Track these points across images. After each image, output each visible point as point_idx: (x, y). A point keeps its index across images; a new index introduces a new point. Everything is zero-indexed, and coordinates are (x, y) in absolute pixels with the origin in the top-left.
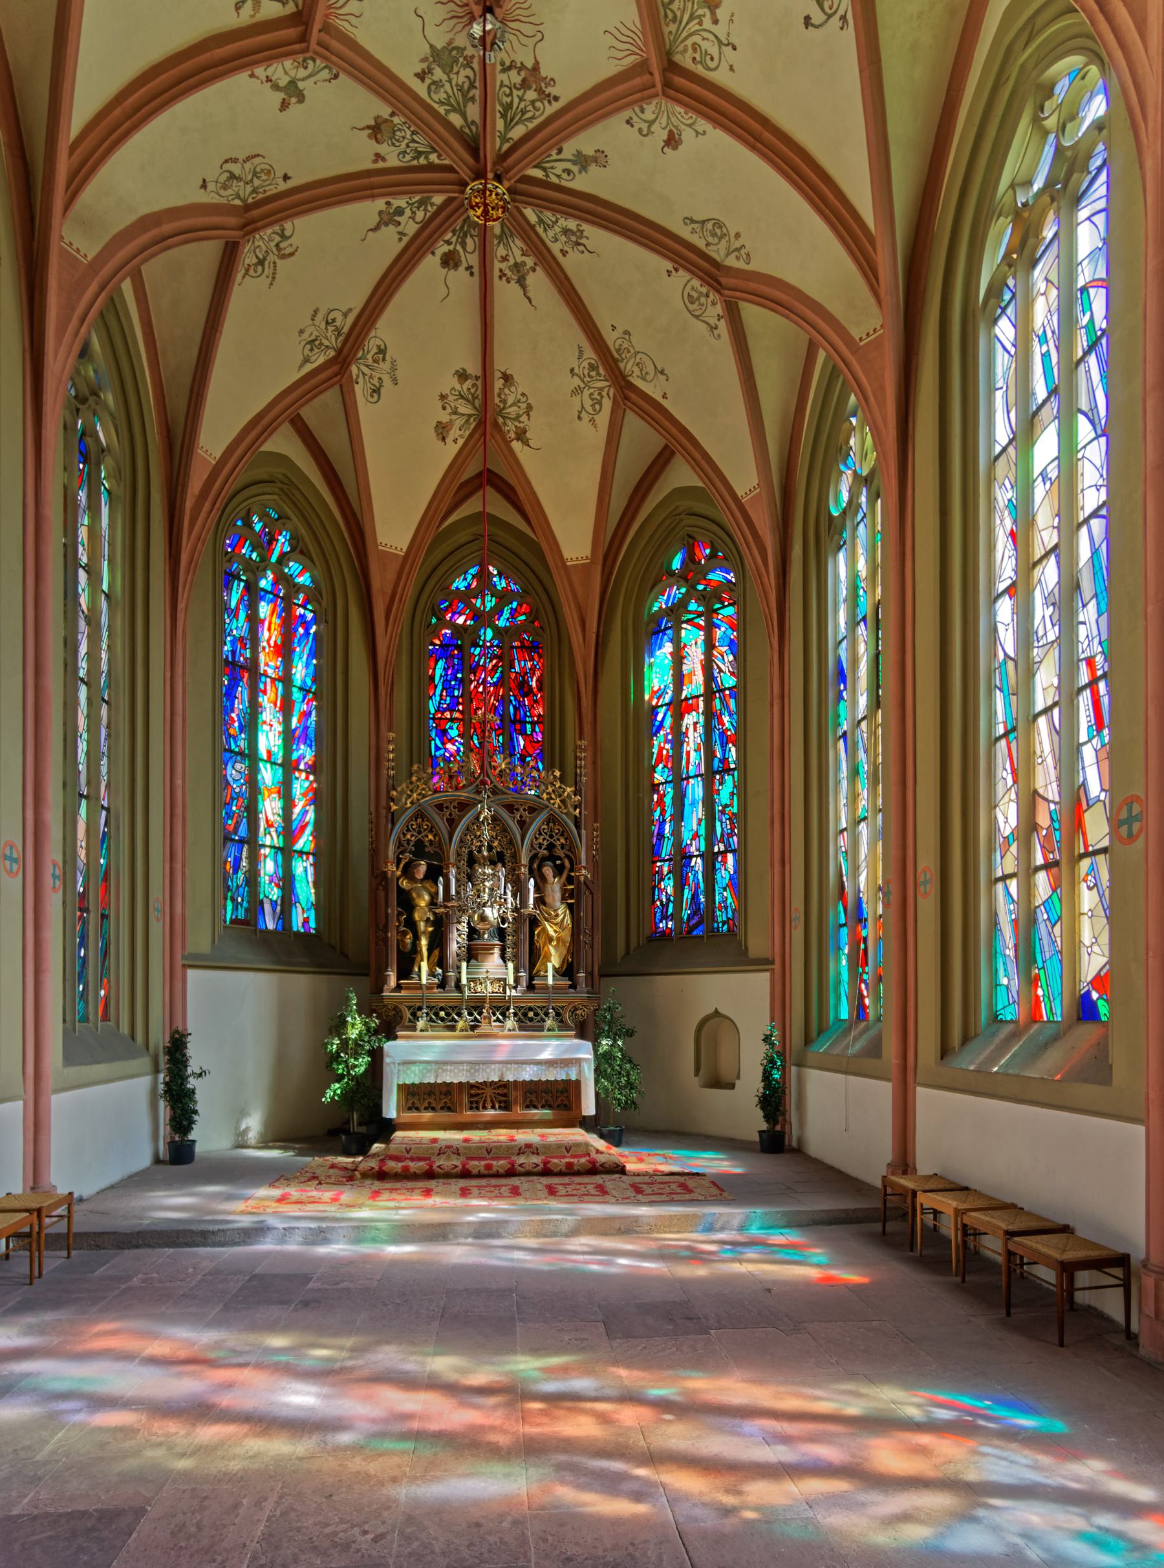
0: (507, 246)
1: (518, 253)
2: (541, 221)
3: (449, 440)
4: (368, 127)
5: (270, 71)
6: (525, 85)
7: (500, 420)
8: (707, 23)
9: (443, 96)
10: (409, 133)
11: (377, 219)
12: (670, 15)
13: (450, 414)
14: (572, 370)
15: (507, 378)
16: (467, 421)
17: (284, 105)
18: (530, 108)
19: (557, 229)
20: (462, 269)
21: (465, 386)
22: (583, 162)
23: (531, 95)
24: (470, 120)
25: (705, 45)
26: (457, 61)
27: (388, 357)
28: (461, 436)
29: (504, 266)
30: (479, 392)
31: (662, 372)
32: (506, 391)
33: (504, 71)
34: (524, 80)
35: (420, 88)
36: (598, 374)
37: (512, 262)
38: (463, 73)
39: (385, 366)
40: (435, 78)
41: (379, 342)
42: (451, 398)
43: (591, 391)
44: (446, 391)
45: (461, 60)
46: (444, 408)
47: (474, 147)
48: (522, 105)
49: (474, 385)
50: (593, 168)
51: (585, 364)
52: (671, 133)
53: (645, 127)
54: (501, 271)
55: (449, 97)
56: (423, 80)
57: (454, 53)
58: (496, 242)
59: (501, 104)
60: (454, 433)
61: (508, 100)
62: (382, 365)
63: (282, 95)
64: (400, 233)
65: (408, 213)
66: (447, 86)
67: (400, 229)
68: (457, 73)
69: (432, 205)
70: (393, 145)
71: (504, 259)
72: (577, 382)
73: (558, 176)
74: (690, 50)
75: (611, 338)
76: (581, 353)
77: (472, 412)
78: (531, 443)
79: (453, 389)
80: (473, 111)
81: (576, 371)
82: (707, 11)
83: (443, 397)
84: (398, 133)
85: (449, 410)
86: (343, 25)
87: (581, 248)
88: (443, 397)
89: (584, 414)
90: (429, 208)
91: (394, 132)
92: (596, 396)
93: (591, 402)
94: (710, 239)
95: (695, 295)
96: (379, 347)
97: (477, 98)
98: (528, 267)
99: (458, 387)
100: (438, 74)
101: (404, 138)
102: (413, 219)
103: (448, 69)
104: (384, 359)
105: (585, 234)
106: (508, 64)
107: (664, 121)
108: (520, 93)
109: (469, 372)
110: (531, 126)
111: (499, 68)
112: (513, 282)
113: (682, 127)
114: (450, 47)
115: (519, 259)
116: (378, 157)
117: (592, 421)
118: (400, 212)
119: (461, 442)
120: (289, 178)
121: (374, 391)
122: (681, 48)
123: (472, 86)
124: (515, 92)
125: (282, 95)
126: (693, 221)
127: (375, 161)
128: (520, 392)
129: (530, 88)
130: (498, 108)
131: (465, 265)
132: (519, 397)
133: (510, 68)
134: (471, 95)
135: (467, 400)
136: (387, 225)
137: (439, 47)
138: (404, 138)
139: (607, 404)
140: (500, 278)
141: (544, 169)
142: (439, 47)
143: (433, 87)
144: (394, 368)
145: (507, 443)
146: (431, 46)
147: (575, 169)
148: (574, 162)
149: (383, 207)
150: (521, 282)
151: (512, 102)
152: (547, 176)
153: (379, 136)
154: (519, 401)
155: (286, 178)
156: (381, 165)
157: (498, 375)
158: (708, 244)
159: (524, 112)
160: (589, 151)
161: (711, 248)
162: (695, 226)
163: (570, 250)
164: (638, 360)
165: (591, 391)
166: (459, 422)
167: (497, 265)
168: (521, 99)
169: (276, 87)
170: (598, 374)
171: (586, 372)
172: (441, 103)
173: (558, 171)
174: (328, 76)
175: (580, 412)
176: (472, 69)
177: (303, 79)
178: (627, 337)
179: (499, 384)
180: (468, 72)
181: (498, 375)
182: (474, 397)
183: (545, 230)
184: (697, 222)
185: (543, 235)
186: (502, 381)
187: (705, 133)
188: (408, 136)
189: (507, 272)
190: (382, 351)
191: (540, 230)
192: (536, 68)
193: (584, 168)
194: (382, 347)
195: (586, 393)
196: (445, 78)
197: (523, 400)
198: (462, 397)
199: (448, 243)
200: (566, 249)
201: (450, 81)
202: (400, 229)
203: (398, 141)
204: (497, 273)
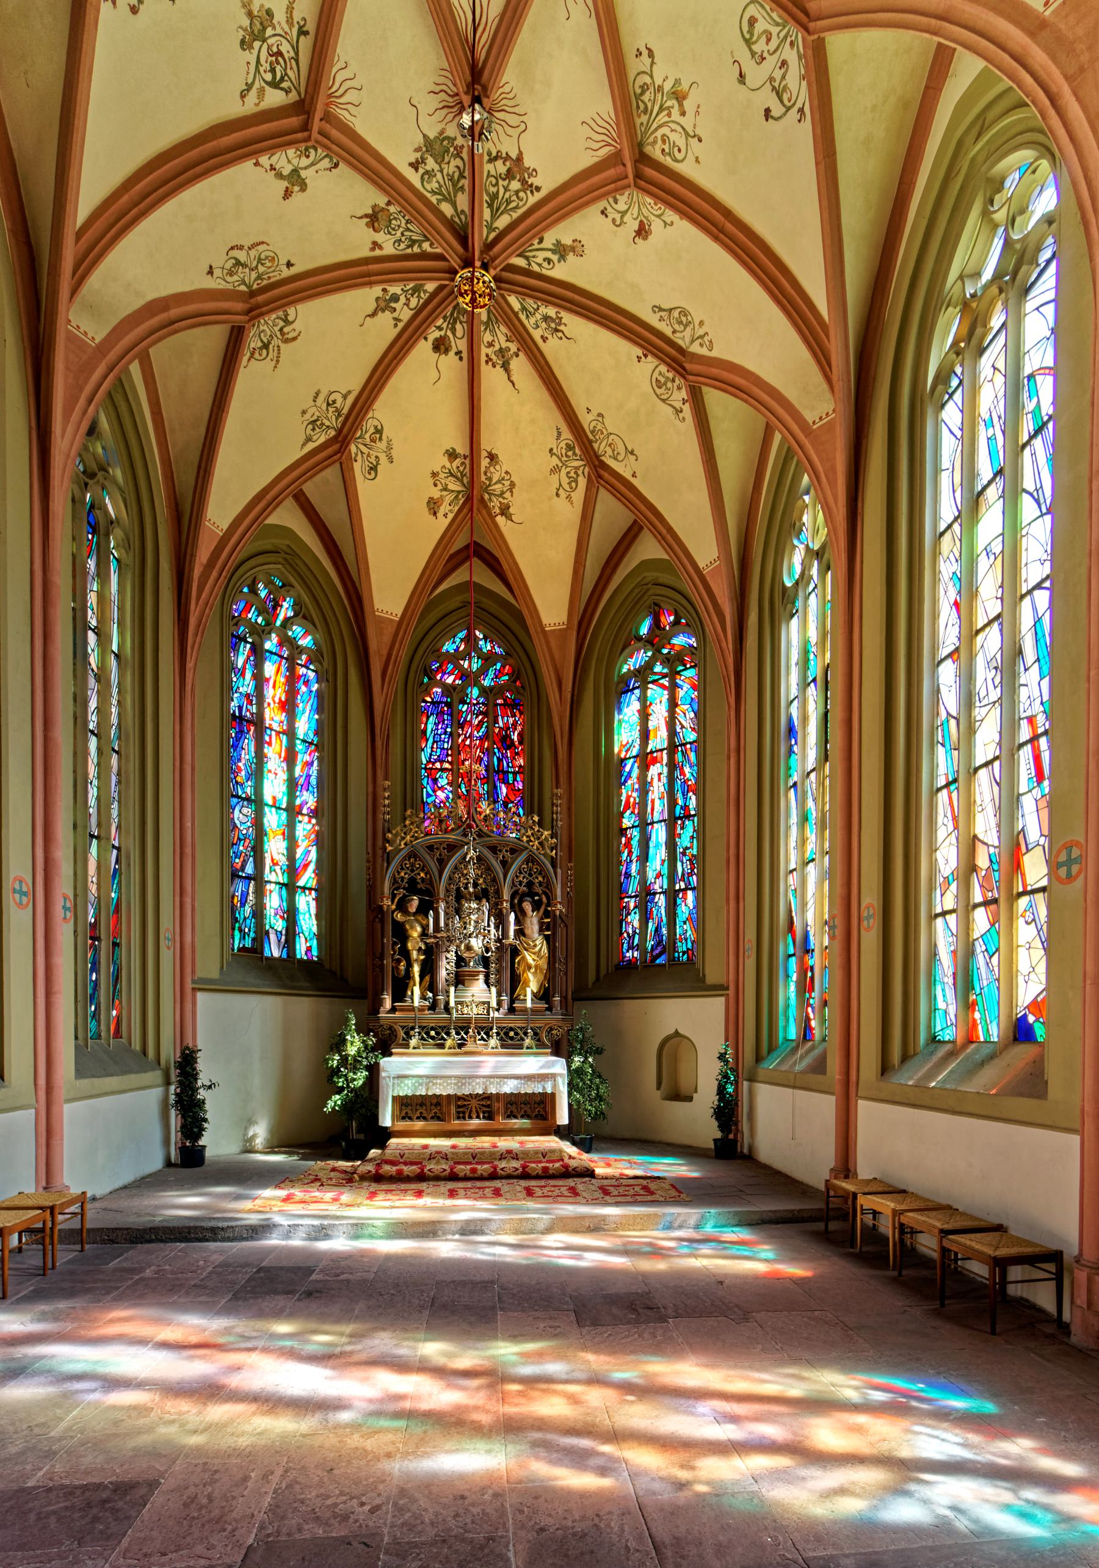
0: (493, 333)
1: (502, 339)
2: (524, 309)
4: (366, 216)
6: (509, 175)
7: (486, 496)
9: (435, 185)
15: (492, 457)
16: (456, 497)
17: (287, 194)
19: (538, 316)
20: (452, 353)
22: (562, 251)
23: (515, 185)
26: (448, 151)
27: (384, 437)
28: (451, 511)
30: (467, 470)
32: (492, 469)
33: (490, 161)
37: (497, 347)
38: (453, 163)
39: (382, 445)
41: (376, 423)
42: (442, 475)
44: (437, 469)
46: (435, 485)
47: (463, 237)
48: (507, 195)
49: (463, 463)
50: (571, 257)
54: (487, 355)
57: (445, 143)
58: (483, 328)
59: (488, 194)
61: (495, 190)
62: (378, 444)
63: (285, 184)
64: (395, 319)
65: (403, 299)
66: (439, 175)
67: (395, 315)
69: (425, 292)
71: (490, 345)
73: (540, 265)
79: (444, 467)
80: (463, 201)
83: (434, 475)
85: (440, 487)
86: (343, 114)
87: (560, 334)
88: (434, 475)
91: (390, 221)
96: (376, 427)
99: (448, 465)
102: (408, 305)
103: (440, 160)
104: (380, 439)
105: (563, 321)
106: (494, 154)
108: (506, 183)
110: (515, 215)
111: (486, 158)
112: (498, 367)
115: (504, 345)
116: (376, 245)
119: (451, 516)
120: (292, 265)
124: (501, 182)
127: (373, 249)
128: (504, 470)
129: (514, 178)
130: (486, 198)
131: (454, 350)
133: (496, 158)
140: (487, 362)
141: (527, 258)
144: (389, 447)
147: (555, 258)
148: (554, 252)
150: (506, 366)
152: (529, 264)
155: (289, 265)
156: (378, 252)
157: (484, 454)
163: (550, 337)
166: (449, 498)
167: (484, 350)
168: (506, 189)
169: (280, 176)
172: (433, 192)
173: (539, 260)
177: (306, 168)
179: (485, 462)
181: (484, 454)
182: (463, 476)
183: (527, 317)
185: (525, 322)
186: (488, 460)
189: (494, 357)
190: (379, 431)
191: (523, 317)
192: (520, 159)
193: (563, 258)
194: (379, 427)
196: (437, 167)
197: (507, 477)
198: (452, 475)
199: (440, 328)
200: (546, 335)
201: (441, 171)
202: (395, 315)
204: (483, 358)
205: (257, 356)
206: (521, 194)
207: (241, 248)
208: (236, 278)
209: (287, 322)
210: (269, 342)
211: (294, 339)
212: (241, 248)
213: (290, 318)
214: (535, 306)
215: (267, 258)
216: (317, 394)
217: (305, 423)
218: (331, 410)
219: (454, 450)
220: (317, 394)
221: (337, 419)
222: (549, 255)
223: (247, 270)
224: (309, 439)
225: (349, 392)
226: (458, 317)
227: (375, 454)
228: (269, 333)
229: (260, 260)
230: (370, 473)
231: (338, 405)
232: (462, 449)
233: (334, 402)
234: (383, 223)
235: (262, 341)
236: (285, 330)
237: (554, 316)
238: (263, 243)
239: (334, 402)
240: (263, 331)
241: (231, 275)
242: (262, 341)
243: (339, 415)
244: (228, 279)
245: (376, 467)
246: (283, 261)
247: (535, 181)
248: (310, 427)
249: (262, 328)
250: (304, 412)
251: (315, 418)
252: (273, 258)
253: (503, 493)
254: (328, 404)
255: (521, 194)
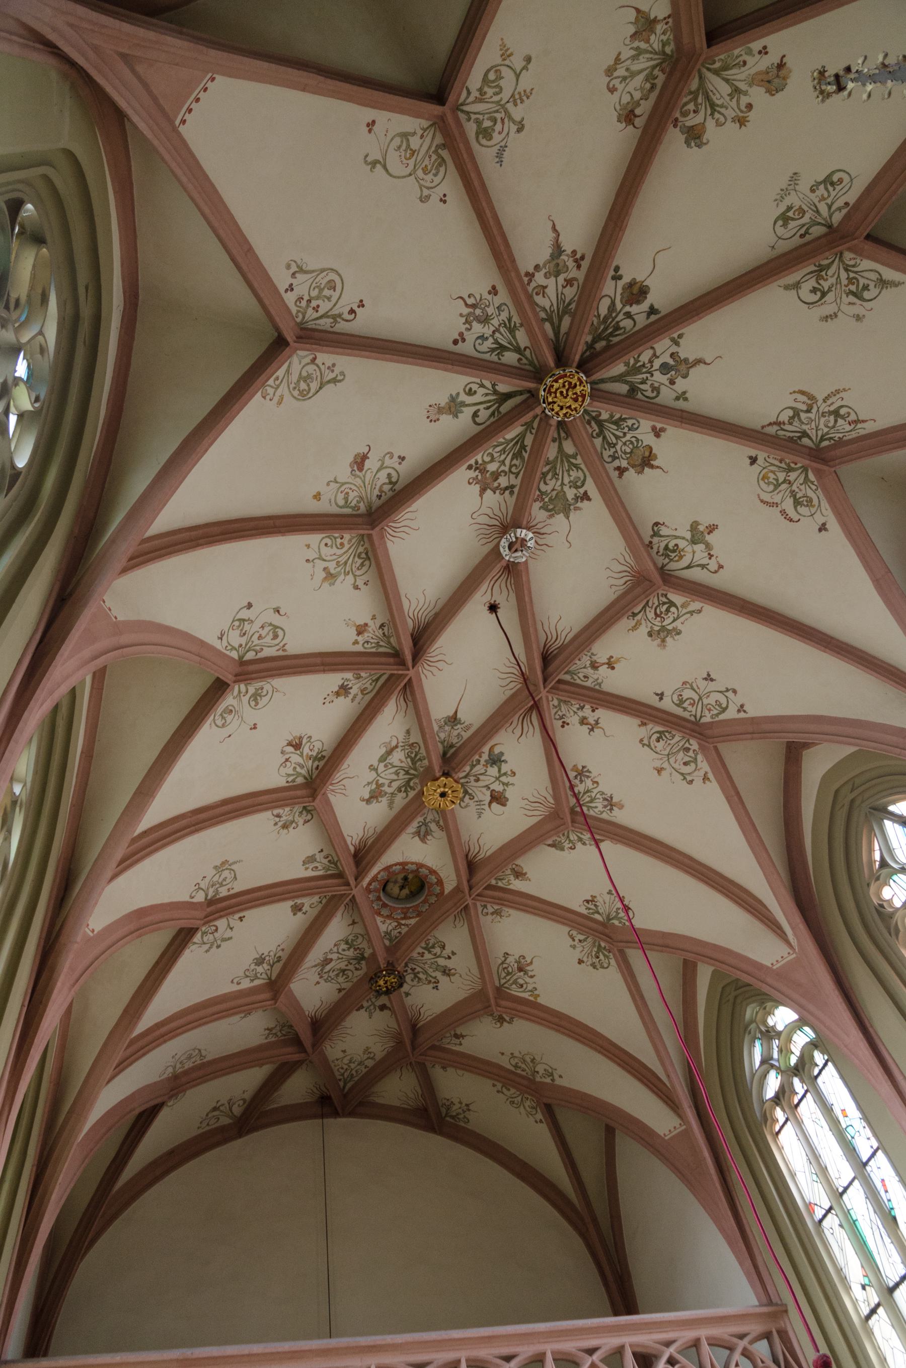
0: (560, 297)
1: (551, 291)
2: (512, 331)
3: (773, 58)
4: (652, 467)
5: (705, 561)
6: (496, 475)
8: (332, 566)
9: (574, 474)
10: (618, 447)
11: (692, 371)
12: (363, 555)
13: (746, 93)
14: (519, 131)
15: (628, 117)
16: (726, 68)
18: (496, 455)
19: (495, 322)
20: (626, 279)
21: (698, 119)
22: (454, 407)
23: (492, 467)
24: (557, 444)
25: (335, 550)
26: (551, 500)
27: (782, 208)
28: (750, 52)
29: (573, 273)
31: (374, 163)
32: (637, 95)
33: (513, 487)
34: (496, 479)
35: (590, 487)
36: (478, 122)
37: (561, 279)
38: (548, 488)
39: (793, 200)
40: (574, 491)
41: (780, 231)
42: (730, 113)
43: (496, 98)
44: (731, 127)
45: (547, 500)
46: (750, 106)
48: (503, 457)
49: (685, 114)
50: (443, 401)
51: (497, 138)
52: (361, 469)
53: (388, 462)
54: (579, 267)
55: (568, 471)
56: (586, 493)
57: (551, 507)
58: (573, 306)
59: (523, 458)
60: (758, 64)
61: (515, 462)
62: (797, 204)
63: (708, 538)
64: (677, 344)
65: (657, 364)
66: (566, 481)
67: (674, 349)
68: (553, 490)
69: (627, 364)
70: (638, 440)
71: (569, 282)
72: (517, 112)
73: (482, 386)
74: (346, 543)
75: (449, 183)
76: (500, 155)
77: (709, 75)
78: (633, 13)
79: (719, 124)
80: (551, 452)
81: (514, 128)
82: (332, 571)
83: (742, 122)
84: (628, 450)
85: (744, 100)
87: (470, 301)
88: (742, 122)
89: (518, 64)
90: (632, 362)
91: (631, 453)
92: (490, 92)
93: (502, 83)
94: (311, 368)
95: (327, 292)
96: (785, 225)
97: (542, 463)
98: (544, 271)
99: (710, 124)
100: (570, 493)
101: (625, 444)
102: (655, 355)
103: (561, 495)
104: (789, 208)
105: (464, 320)
106: (507, 492)
107: (369, 476)
108: (503, 468)
109: (683, 138)
111: (516, 490)
112: (569, 252)
113: (350, 480)
114: (552, 512)
116: (657, 433)
117: (506, 54)
118: (665, 368)
119: (756, 46)
120: (751, 458)
121: (832, 184)
122: (354, 541)
123: (544, 475)
124: (507, 469)
125: (708, 538)
126: (334, 381)
127: (663, 430)
128: (617, 95)
129: (493, 473)
130: (526, 455)
131: (621, 284)
132: (620, 87)
133: (506, 488)
134: (548, 467)
135: (708, 98)
136: (686, 360)
137: (562, 514)
138: (625, 444)
139: (474, 80)
140: (582, 258)
141: (495, 392)
142: (562, 514)
143: (579, 484)
144: (784, 193)
145: (675, 15)
146: (568, 518)
147: (463, 397)
148: (463, 404)
149: (679, 381)
151: (512, 459)
152: (494, 385)
153: (647, 454)
154: (624, 78)
155: (753, 460)
157: (639, 122)
158: (313, 360)
159: (504, 450)
160: (446, 419)
161: (308, 360)
162: (332, 376)
163: (486, 295)
164: (411, 162)
165: (496, 98)
166: (739, 75)
167: (580, 275)
168: (503, 463)
169: (708, 546)
170: (478, 122)
171: (498, 127)
172: (577, 467)
174: (663, 528)
175: (525, 68)
176: (539, 490)
177: (683, 538)
178: (426, 192)
179: (644, 109)
180: (543, 487)
181: (639, 122)
182: (695, 95)
183: (510, 320)
184: (329, 382)
185: (514, 313)
186: (638, 111)
187: (328, 484)
188: (620, 444)
189: (571, 264)
190: (784, 219)
191: (516, 319)
192: (483, 491)
193: (453, 399)
194: (780, 223)
195: (506, 95)
196: (566, 489)
197: (616, 82)
198: (713, 106)
199: (628, 315)
200: (489, 297)
201: (563, 484)
202: (674, 349)
203: (632, 443)
204: (585, 264)
205: (853, 417)
206: (487, 459)
207: (783, 512)
208: (810, 493)
209: (796, 413)
210: (830, 413)
211: (803, 393)
212: (783, 512)
213: (790, 413)
214: (497, 335)
215: (769, 484)
216: (826, 318)
217: (868, 305)
218: (826, 285)
219: (687, 143)
220: (826, 318)
221: (828, 266)
222: (469, 400)
223: (794, 487)
224: (883, 283)
225: (787, 288)
226: (600, 323)
227: (812, 196)
228: (823, 420)
229: (777, 486)
230: (841, 181)
231: (812, 283)
232: (674, 138)
233: (814, 291)
234: (639, 453)
235: (836, 421)
236: (804, 408)
237: (475, 324)
238: (762, 501)
239: (814, 291)
240: (827, 426)
241: (811, 500)
242: (836, 421)
243: (822, 268)
244: (815, 502)
245: (824, 181)
246: (756, 468)
247: (472, 474)
248: (866, 295)
249: (826, 430)
250: (858, 318)
251: (852, 299)
252: (763, 479)
253: (634, 58)
254: (824, 294)
255: (487, 459)
